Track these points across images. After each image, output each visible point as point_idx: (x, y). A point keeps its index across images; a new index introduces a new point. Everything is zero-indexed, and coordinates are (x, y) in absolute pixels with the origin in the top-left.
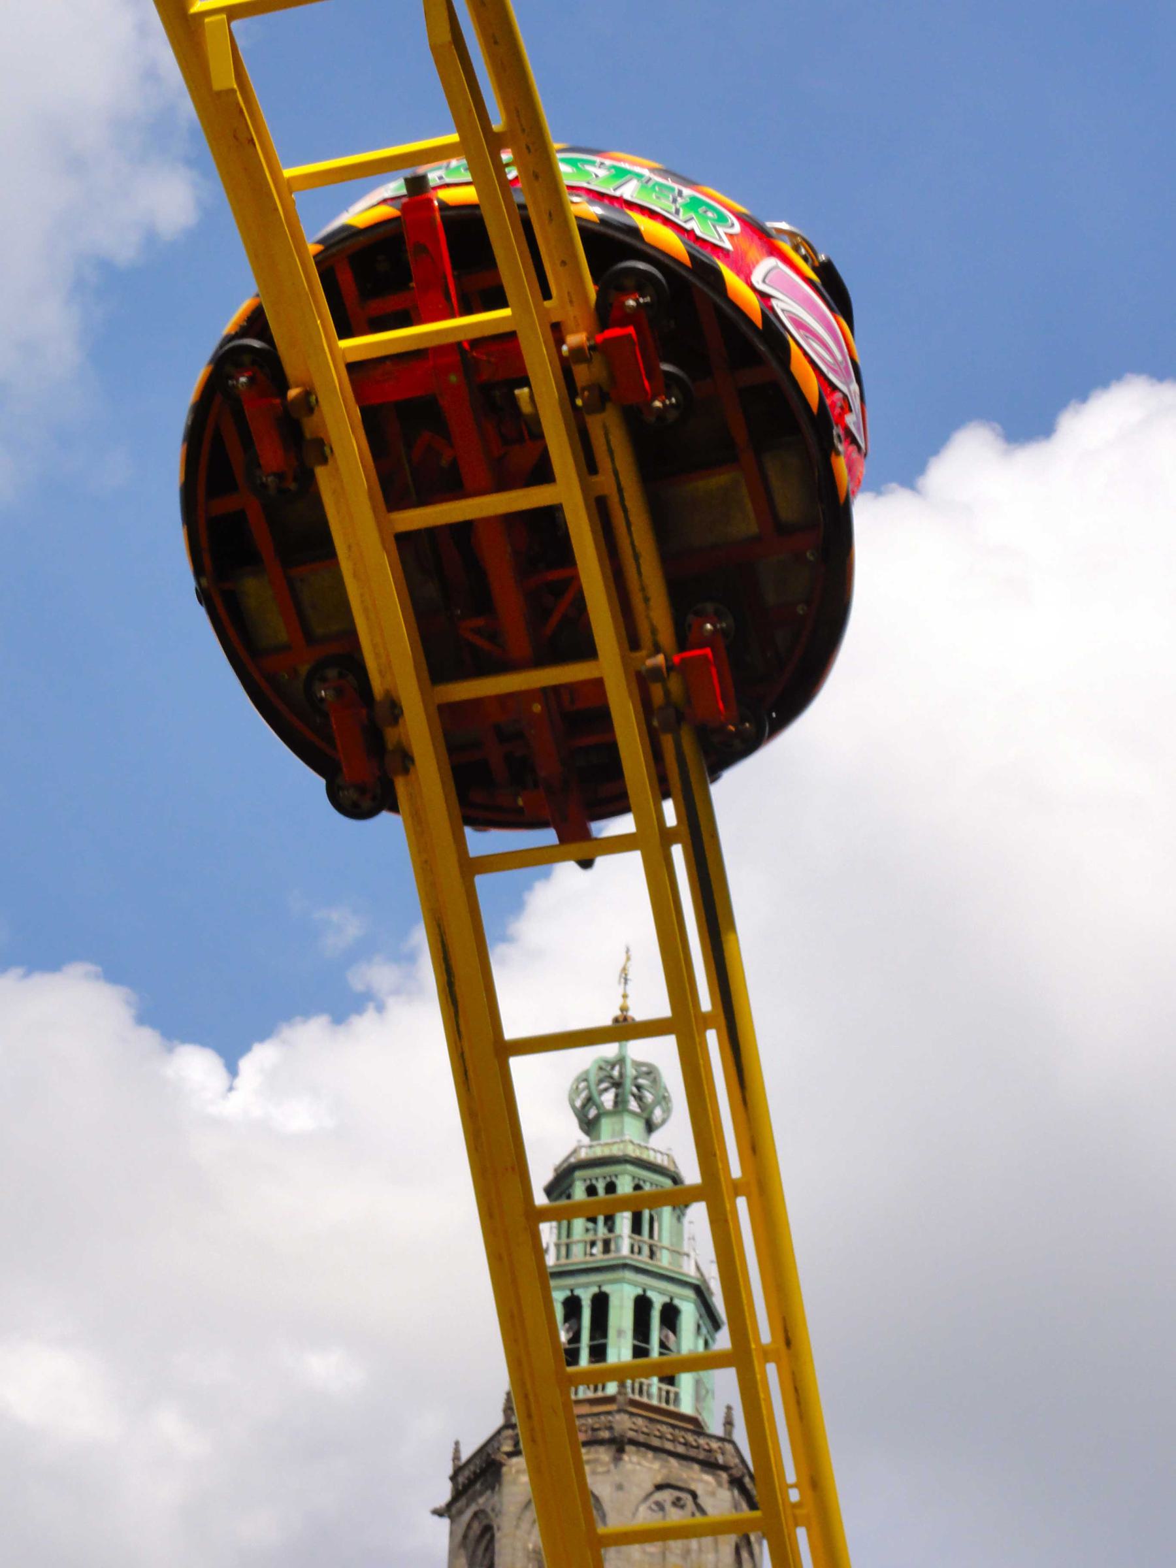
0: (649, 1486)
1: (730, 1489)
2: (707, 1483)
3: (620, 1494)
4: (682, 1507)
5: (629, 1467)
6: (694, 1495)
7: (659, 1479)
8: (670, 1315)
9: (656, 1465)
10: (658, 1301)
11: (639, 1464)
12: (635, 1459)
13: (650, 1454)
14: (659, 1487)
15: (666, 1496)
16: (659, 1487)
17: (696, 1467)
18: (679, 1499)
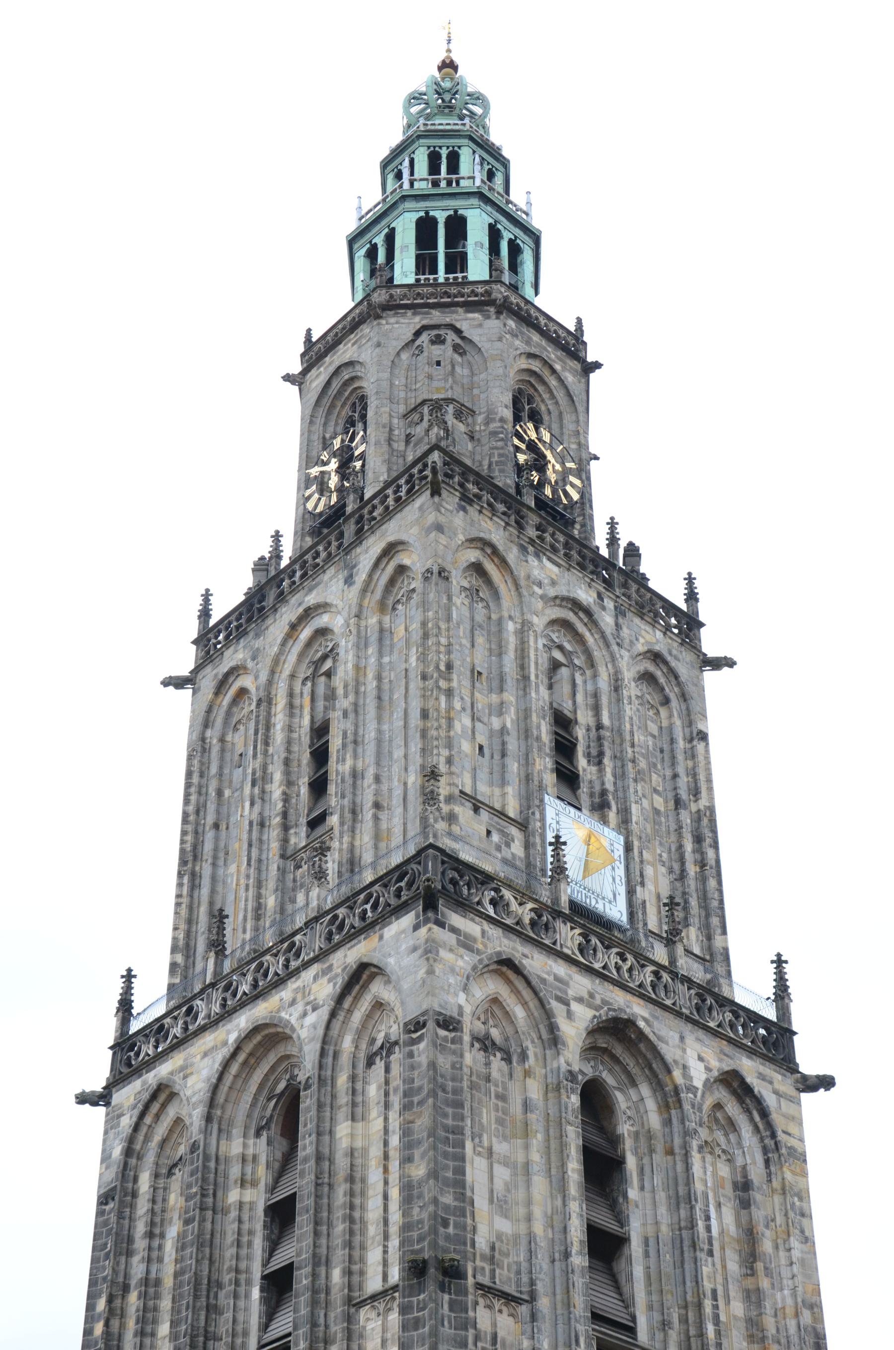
0: (409, 336)
1: (498, 318)
2: (473, 319)
3: (377, 350)
4: (443, 342)
5: (387, 327)
6: (458, 332)
7: (418, 327)
8: (457, 227)
9: (417, 319)
10: (441, 217)
11: (397, 323)
12: (392, 320)
13: (409, 313)
14: (418, 334)
15: (425, 338)
16: (418, 334)
17: (460, 310)
18: (438, 336)
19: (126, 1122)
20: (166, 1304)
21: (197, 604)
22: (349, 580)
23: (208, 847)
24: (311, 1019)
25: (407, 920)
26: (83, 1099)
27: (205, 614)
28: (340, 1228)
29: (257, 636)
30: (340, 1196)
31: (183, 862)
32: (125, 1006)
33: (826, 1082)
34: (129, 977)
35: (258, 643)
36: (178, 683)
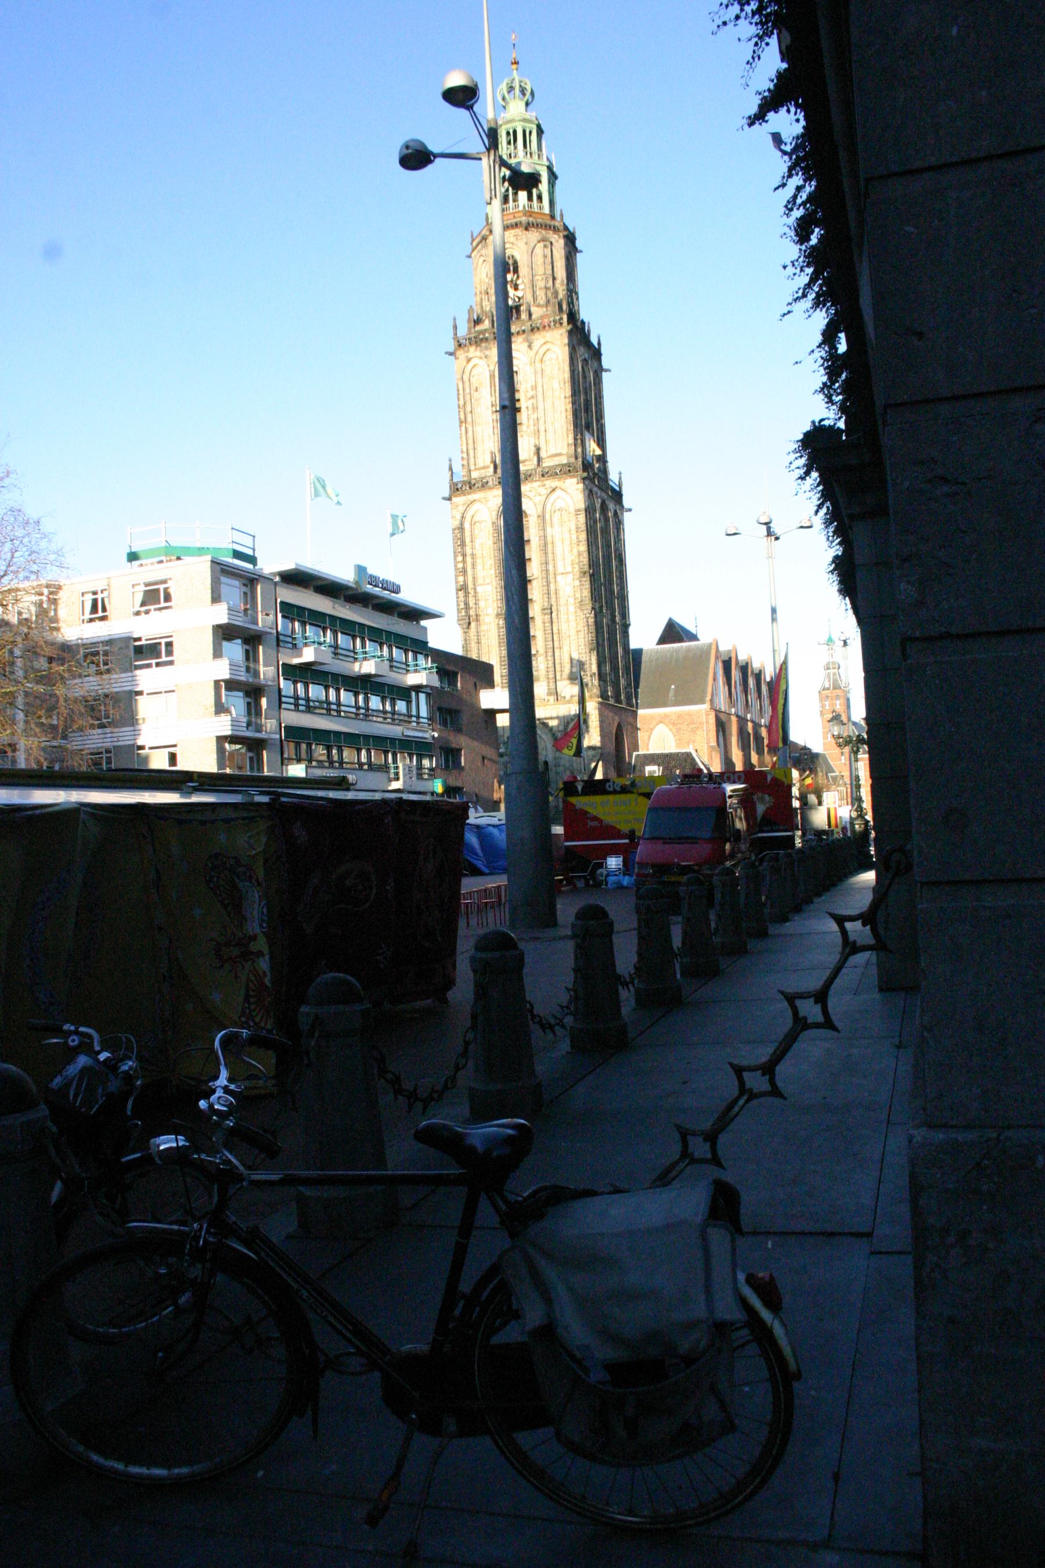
15: (541, 244)
19: (462, 509)
20: (479, 561)
21: (451, 323)
22: (530, 347)
23: (469, 419)
24: (538, 498)
25: (575, 480)
26: (444, 499)
27: (455, 327)
28: (550, 555)
29: (486, 349)
30: (550, 547)
31: (461, 422)
32: (451, 469)
33: (630, 510)
34: (450, 460)
35: (487, 352)
36: (451, 354)
